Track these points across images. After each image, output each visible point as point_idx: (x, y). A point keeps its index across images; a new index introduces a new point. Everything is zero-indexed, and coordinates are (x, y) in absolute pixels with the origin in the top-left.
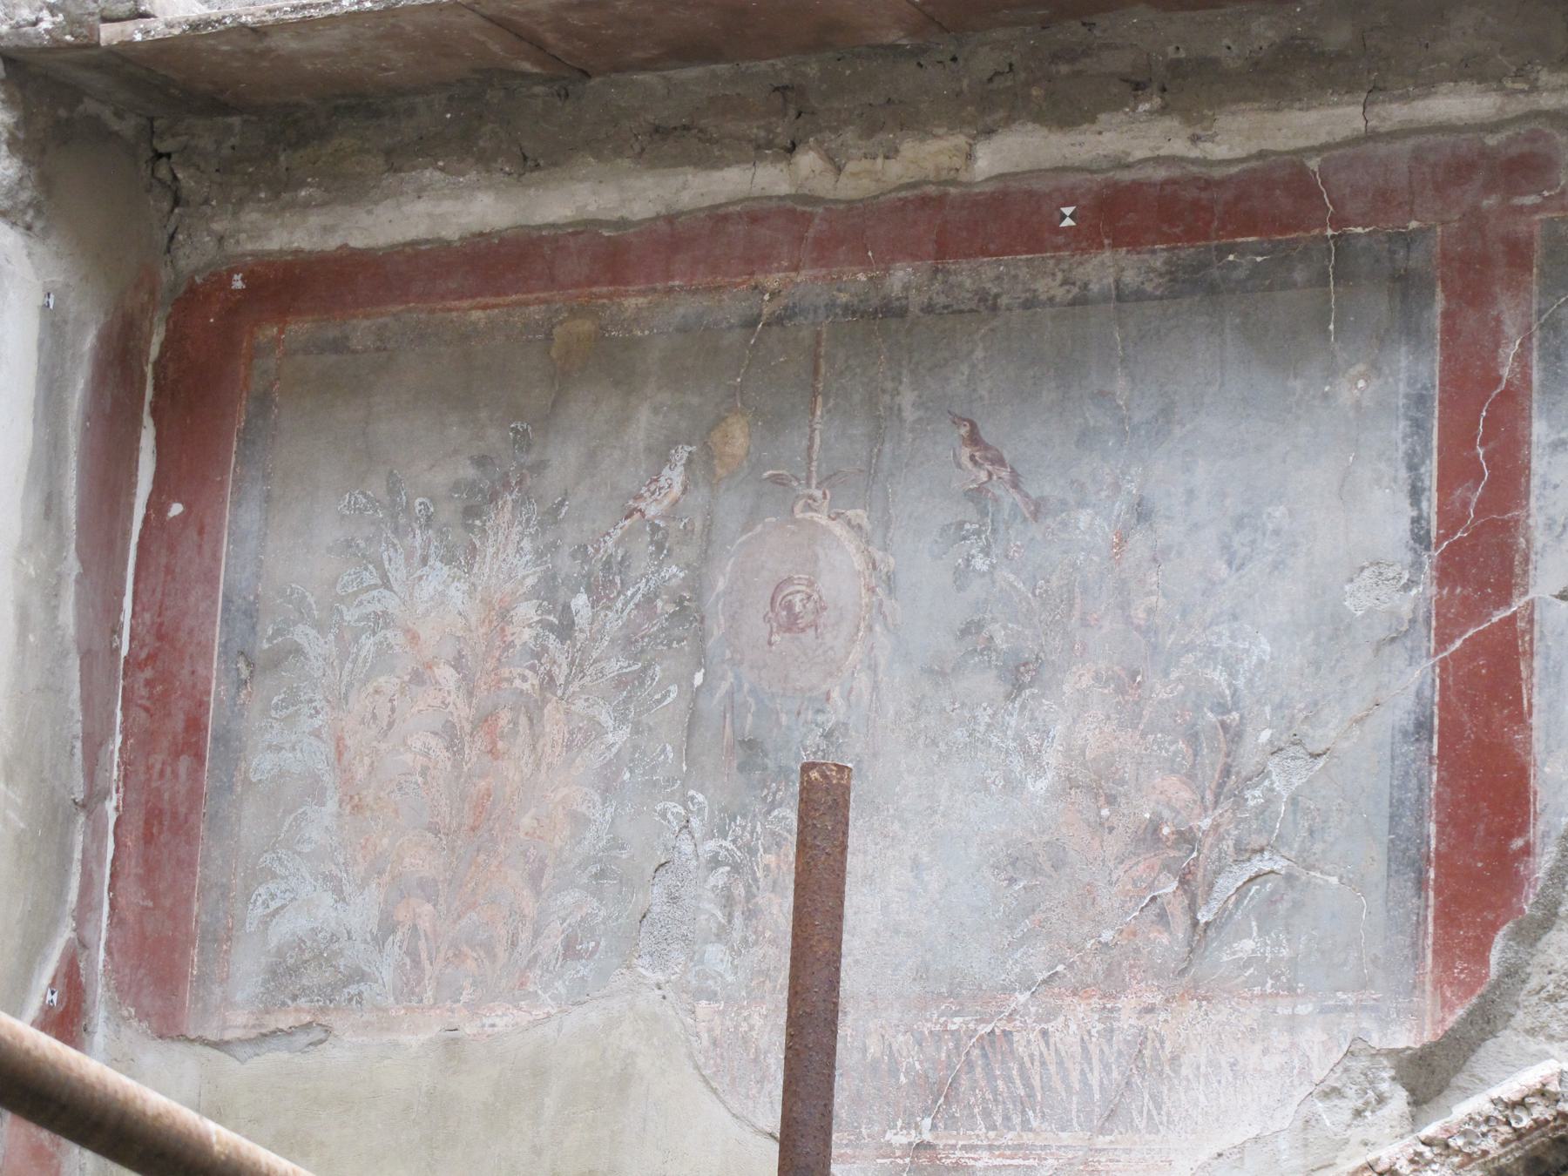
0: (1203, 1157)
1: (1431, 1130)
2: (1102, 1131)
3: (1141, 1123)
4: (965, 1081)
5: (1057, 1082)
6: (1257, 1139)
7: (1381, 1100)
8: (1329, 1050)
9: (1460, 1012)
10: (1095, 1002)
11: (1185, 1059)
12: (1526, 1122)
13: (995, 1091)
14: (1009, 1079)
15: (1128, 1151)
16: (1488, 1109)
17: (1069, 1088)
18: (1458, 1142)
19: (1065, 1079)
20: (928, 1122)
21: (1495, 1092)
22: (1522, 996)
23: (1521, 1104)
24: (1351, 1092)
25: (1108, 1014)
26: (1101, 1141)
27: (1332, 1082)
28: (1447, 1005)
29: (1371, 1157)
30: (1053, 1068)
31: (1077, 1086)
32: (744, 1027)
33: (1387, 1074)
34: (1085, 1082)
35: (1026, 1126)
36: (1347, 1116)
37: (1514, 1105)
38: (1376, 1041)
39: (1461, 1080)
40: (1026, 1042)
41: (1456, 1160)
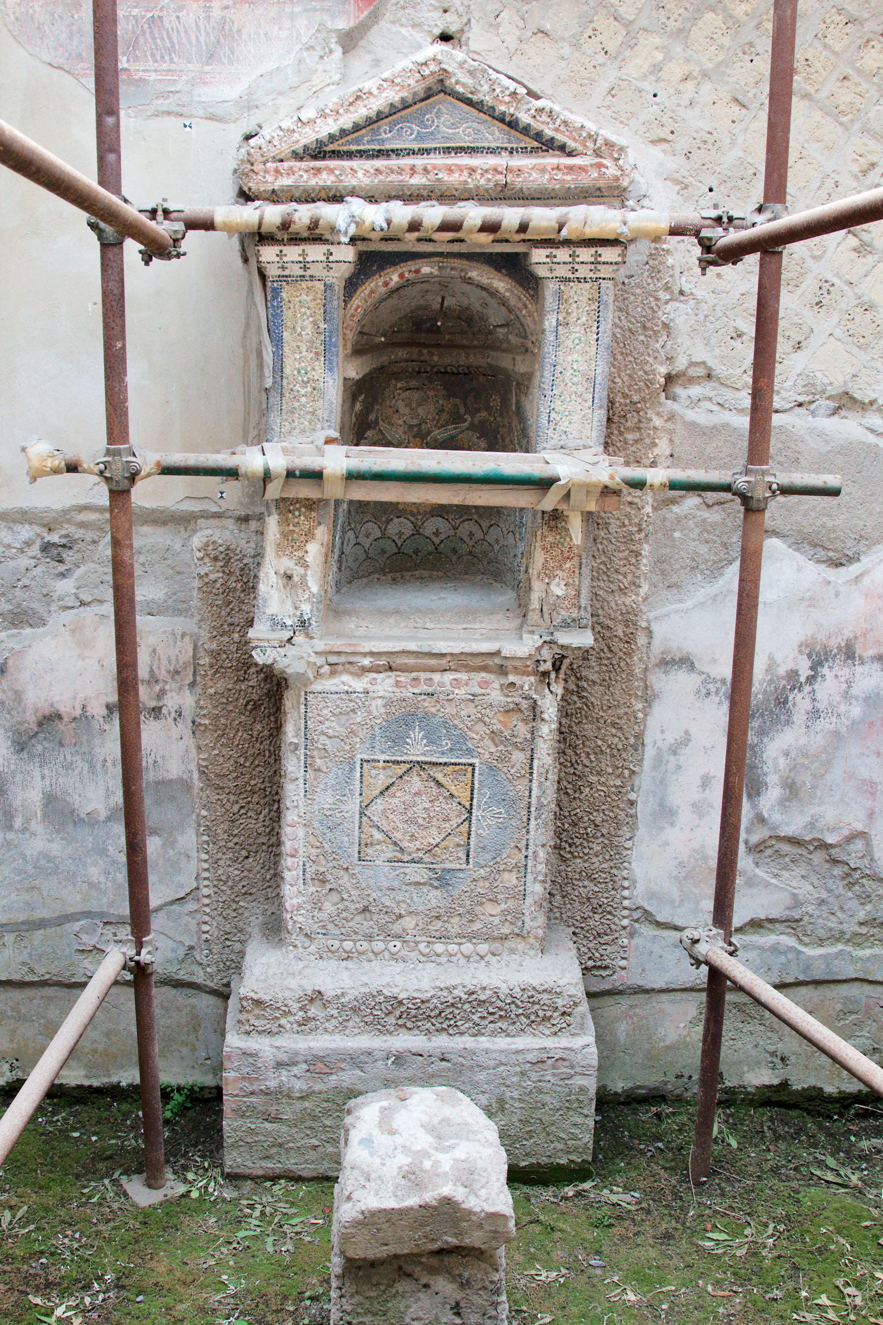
0: (254, 77)
1: (386, 75)
2: (207, 64)
3: (226, 61)
4: (141, 39)
5: (185, 41)
6: (278, 69)
7: (331, 52)
8: (309, 29)
9: (366, 13)
10: (202, 4)
11: (244, 31)
12: (427, 72)
13: (156, 45)
14: (162, 39)
15: (220, 73)
16: (411, 66)
17: (191, 44)
18: (398, 80)
19: (189, 39)
20: (125, 59)
21: (414, 59)
22: (389, 6)
23: (425, 64)
24: (318, 48)
25: (207, 9)
26: (207, 68)
27: (310, 43)
28: (360, 10)
29: (360, 86)
30: (183, 34)
31: (194, 43)
32: (31, 11)
33: (334, 40)
34: (198, 41)
35: (172, 61)
36: (317, 59)
37: (422, 64)
38: (329, 25)
39: (362, 43)
40: (169, 21)
41: (397, 88)
